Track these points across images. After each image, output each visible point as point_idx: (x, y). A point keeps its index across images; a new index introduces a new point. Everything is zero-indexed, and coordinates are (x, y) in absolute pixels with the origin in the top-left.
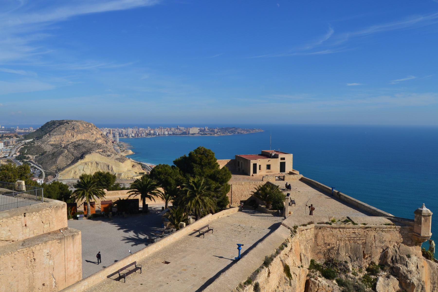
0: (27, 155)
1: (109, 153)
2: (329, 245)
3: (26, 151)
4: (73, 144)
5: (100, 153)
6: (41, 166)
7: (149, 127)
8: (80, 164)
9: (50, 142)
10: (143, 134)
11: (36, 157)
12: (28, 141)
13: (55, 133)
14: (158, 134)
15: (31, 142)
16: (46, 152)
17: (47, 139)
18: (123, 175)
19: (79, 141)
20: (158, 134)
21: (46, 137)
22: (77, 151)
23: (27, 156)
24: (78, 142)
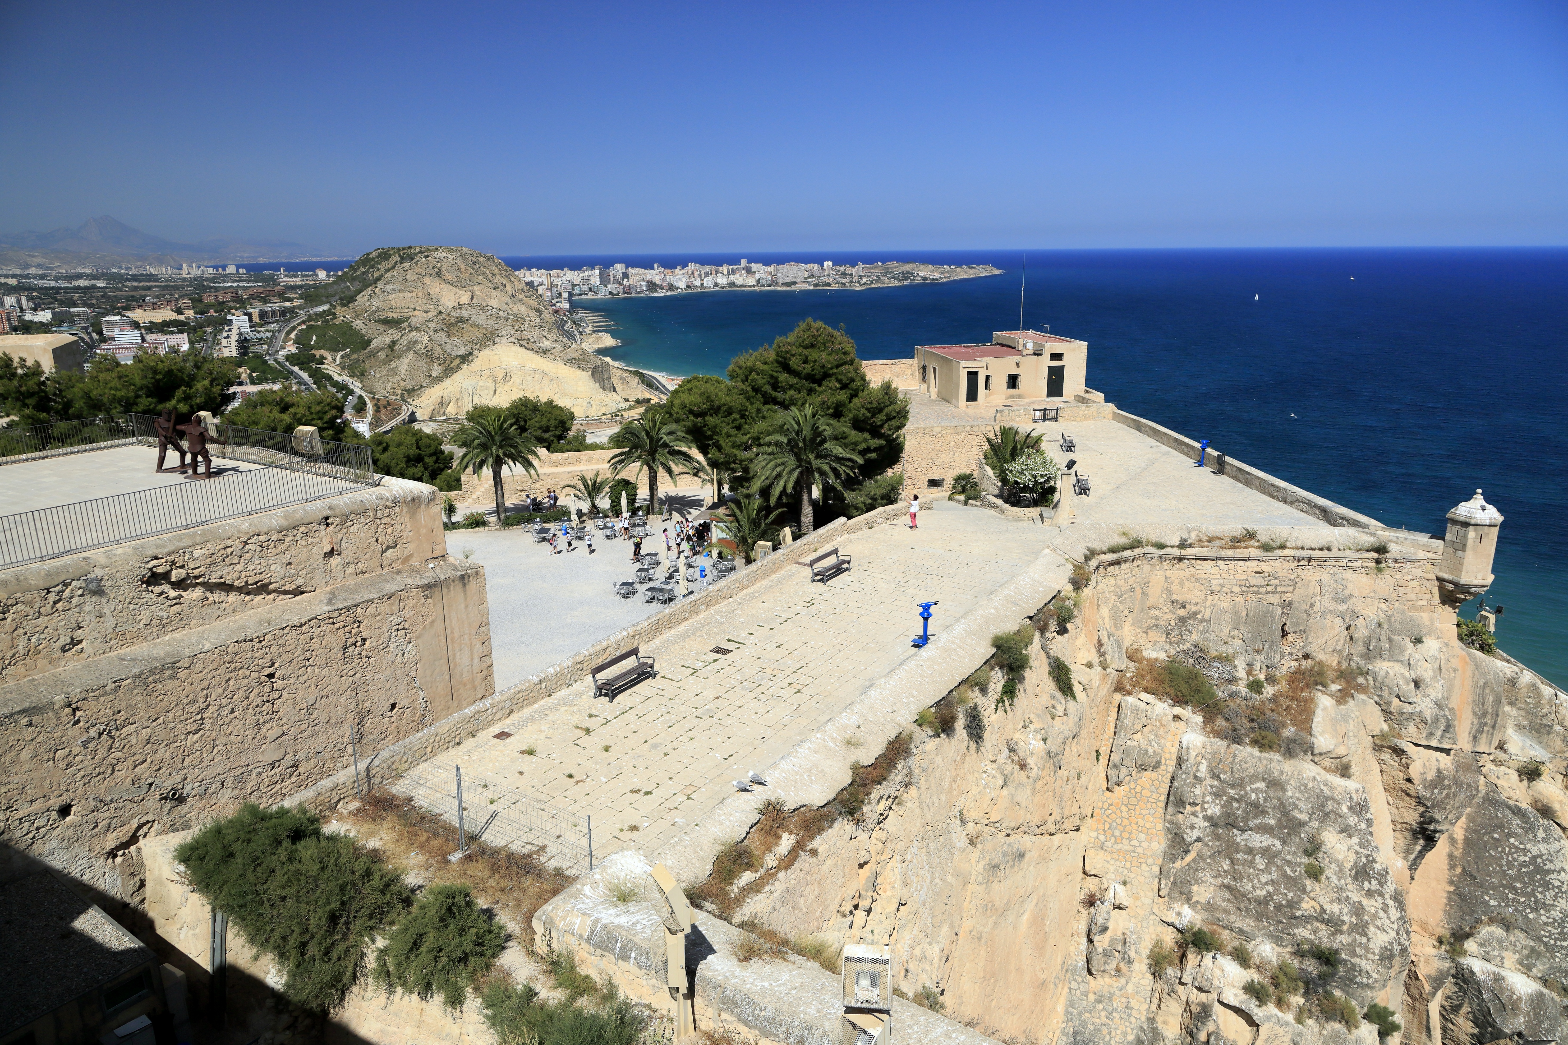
2: (1184, 607)
3: (314, 338)
11: (342, 357)
13: (390, 287)
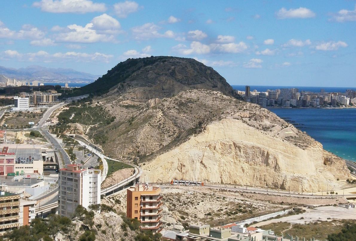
3: (73, 115)
4: (177, 100)
5: (244, 119)
6: (100, 147)
9: (124, 102)
11: (91, 129)
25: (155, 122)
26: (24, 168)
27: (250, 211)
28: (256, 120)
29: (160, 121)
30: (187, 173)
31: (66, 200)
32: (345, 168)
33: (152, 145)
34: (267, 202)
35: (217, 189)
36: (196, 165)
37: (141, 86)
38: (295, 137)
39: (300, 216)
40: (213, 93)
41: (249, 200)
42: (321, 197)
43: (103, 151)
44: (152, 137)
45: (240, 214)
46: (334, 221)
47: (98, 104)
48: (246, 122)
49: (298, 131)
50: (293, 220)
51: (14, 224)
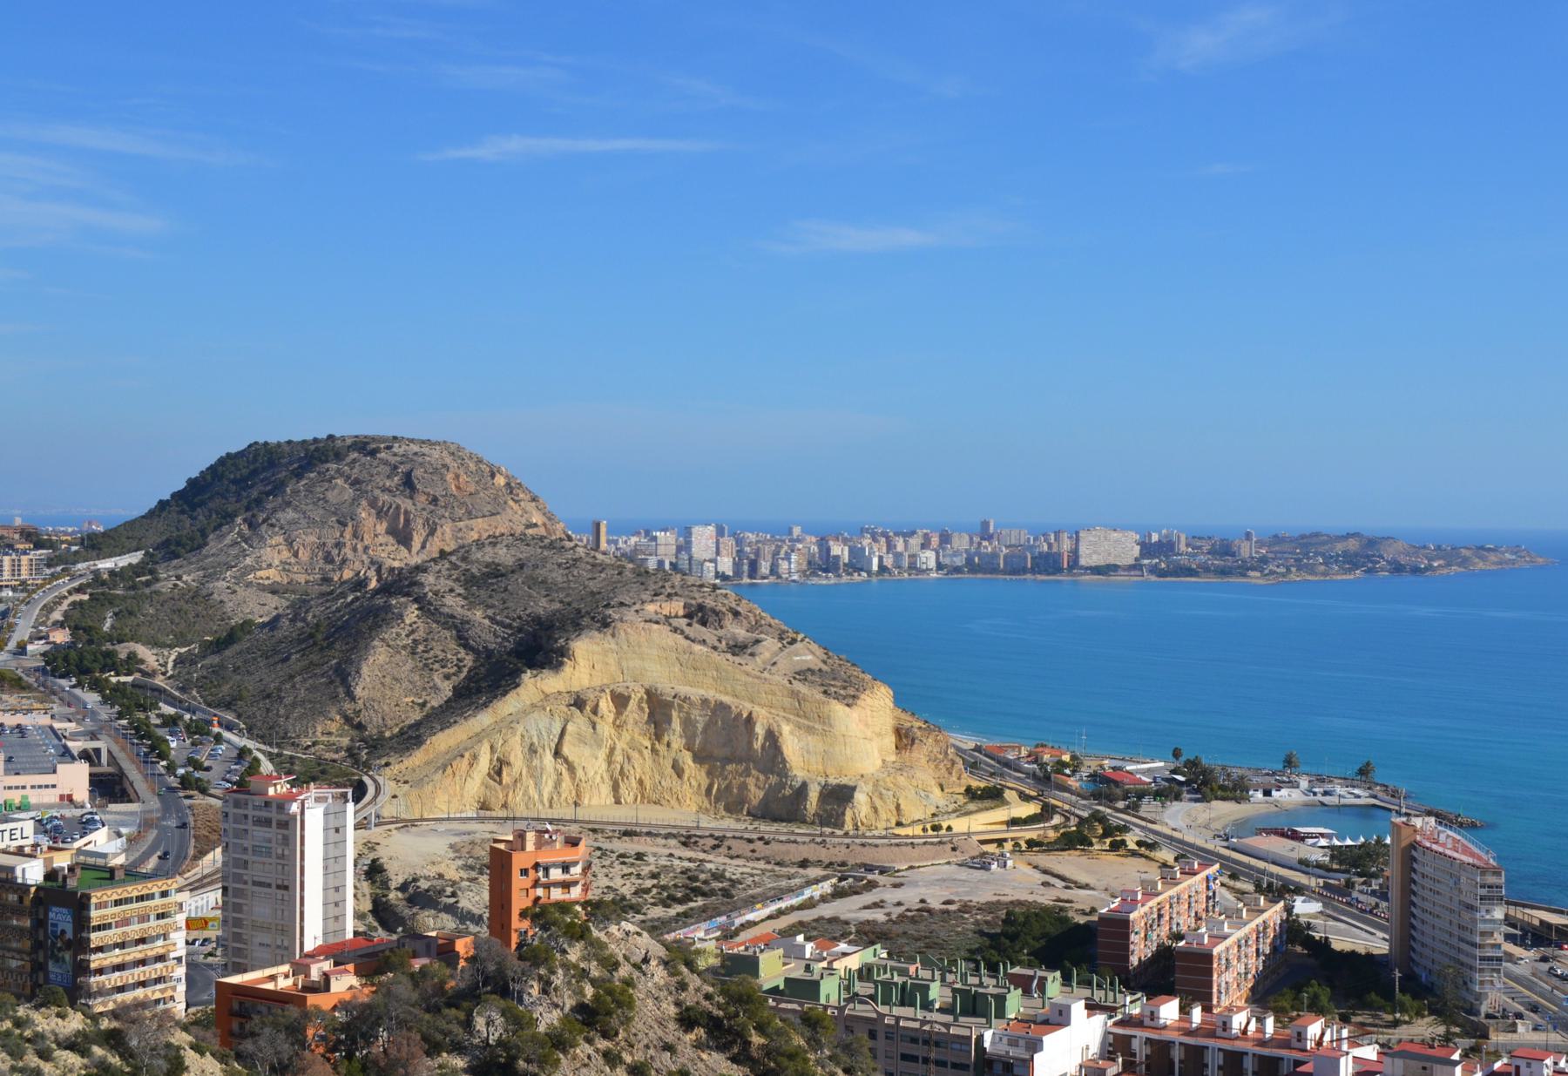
0: (120, 642)
1: (740, 632)
4: (455, 567)
7: (797, 531)
8: (533, 706)
9: (259, 574)
10: (784, 565)
11: (179, 661)
12: (106, 564)
13: (290, 514)
14: (875, 561)
15: (135, 570)
16: (247, 625)
17: (234, 551)
18: (860, 797)
19: (494, 544)
20: (875, 567)
21: (228, 540)
22: (490, 612)
23: (123, 651)
24: (488, 549)
25: (398, 635)
26: (28, 787)
27: (721, 889)
28: (704, 623)
29: (413, 632)
30: (519, 785)
31: (250, 882)
32: (950, 756)
33: (397, 705)
34: (762, 862)
35: (614, 831)
36: (541, 762)
37: (309, 527)
38: (820, 670)
39: (868, 898)
40: (563, 547)
41: (710, 857)
42: (909, 841)
43: (242, 726)
44: (396, 680)
45: (700, 902)
46: (966, 908)
47: (178, 582)
48: (682, 632)
49: (826, 654)
50: (850, 911)
51: (159, 966)
